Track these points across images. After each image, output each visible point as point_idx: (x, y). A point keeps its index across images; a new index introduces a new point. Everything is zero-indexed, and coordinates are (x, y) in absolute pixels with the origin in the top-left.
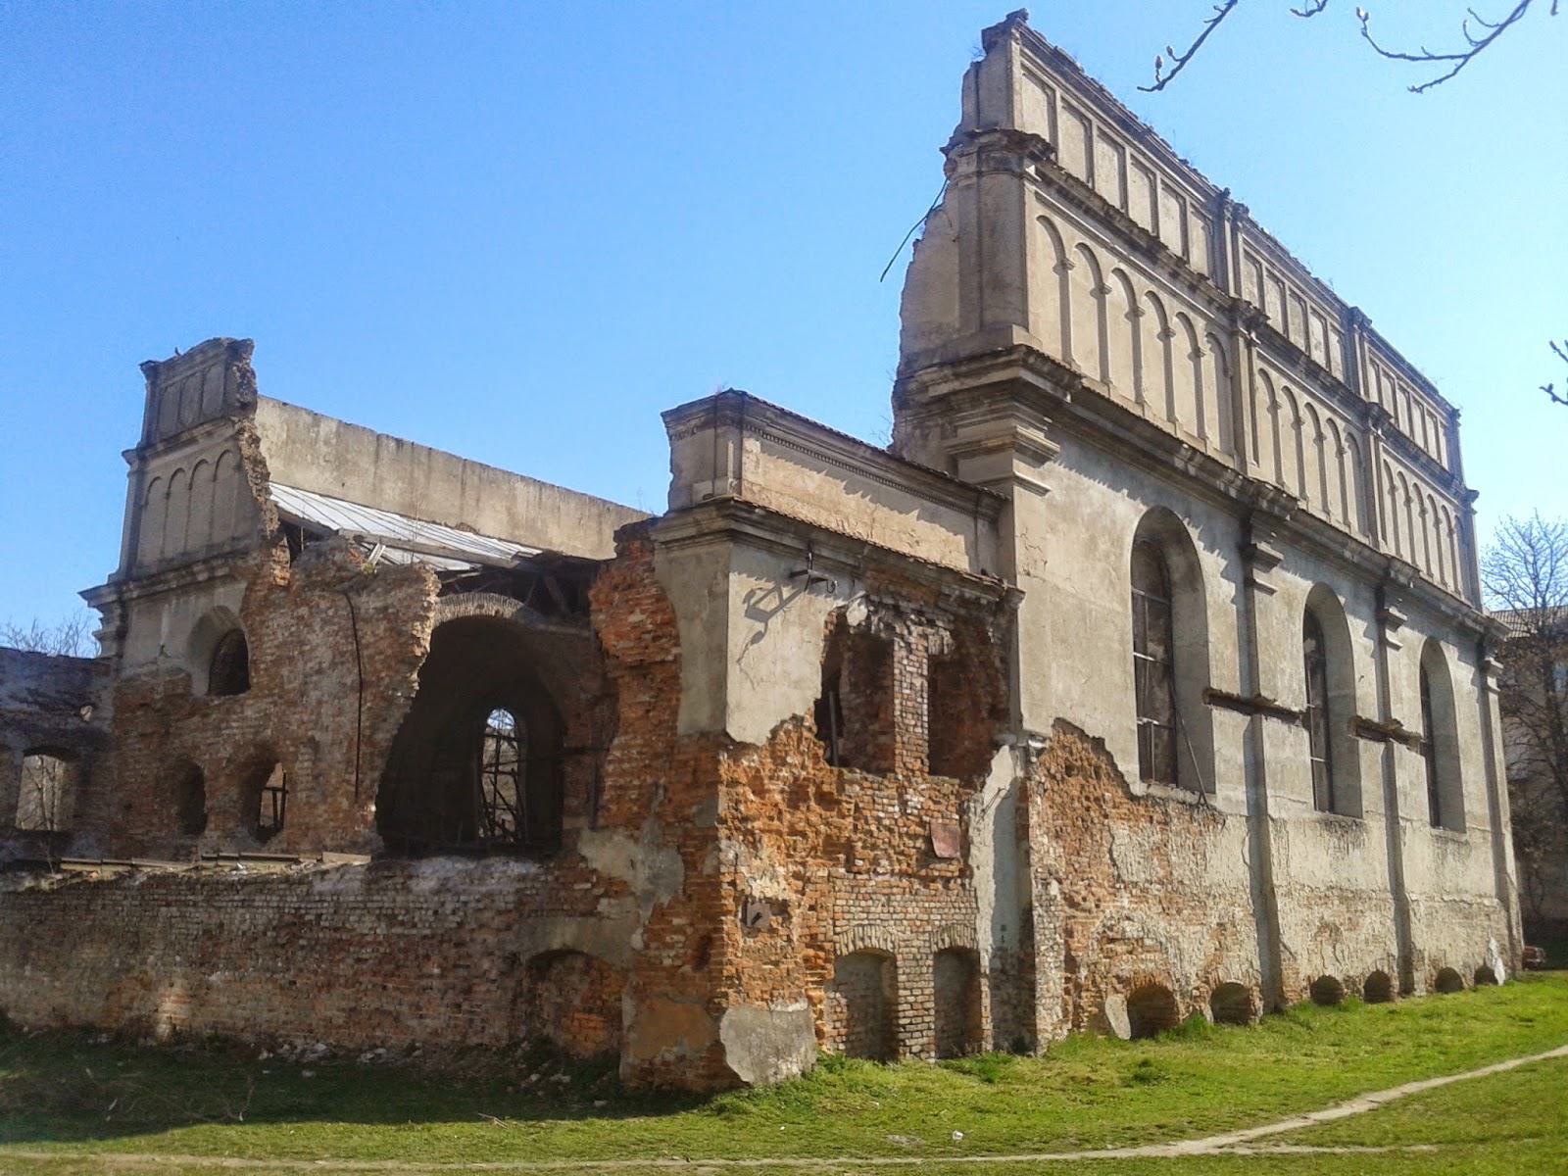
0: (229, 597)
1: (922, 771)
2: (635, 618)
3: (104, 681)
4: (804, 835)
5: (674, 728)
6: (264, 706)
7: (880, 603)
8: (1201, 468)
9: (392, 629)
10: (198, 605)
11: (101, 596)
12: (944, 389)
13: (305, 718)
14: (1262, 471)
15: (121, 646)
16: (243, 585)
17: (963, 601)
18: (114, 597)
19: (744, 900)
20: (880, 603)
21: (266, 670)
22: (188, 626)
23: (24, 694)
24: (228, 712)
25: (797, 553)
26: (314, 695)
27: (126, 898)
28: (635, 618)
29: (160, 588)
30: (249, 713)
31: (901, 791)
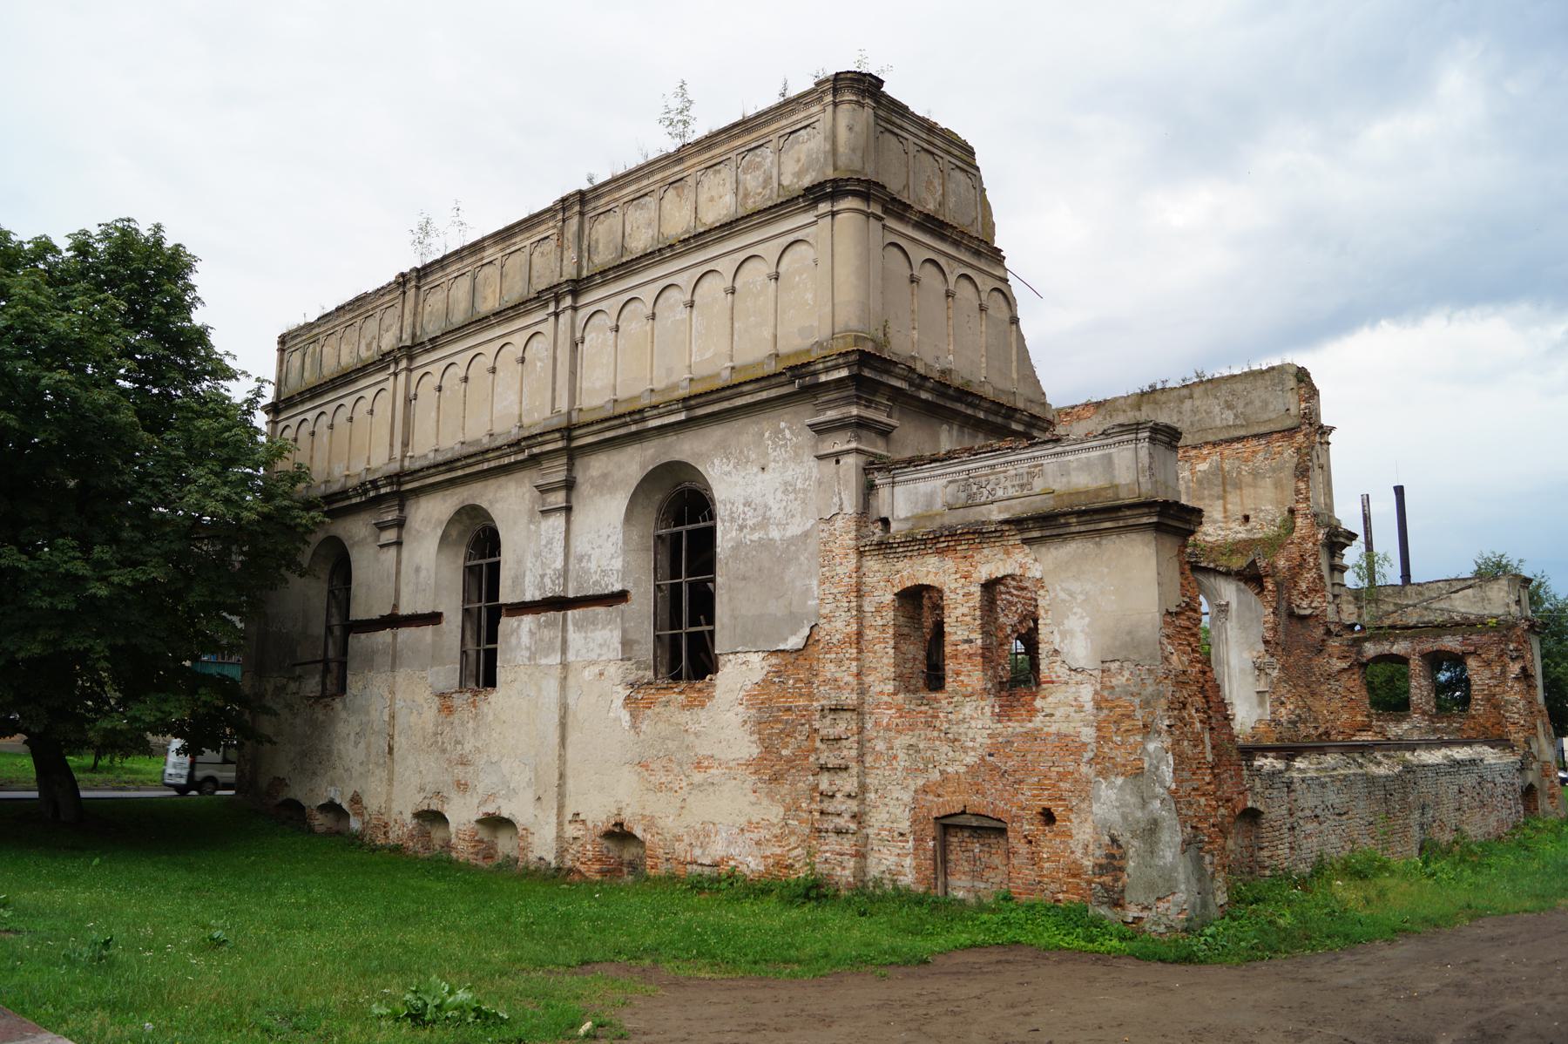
11: (889, 373)
18: (904, 385)
29: (961, 407)
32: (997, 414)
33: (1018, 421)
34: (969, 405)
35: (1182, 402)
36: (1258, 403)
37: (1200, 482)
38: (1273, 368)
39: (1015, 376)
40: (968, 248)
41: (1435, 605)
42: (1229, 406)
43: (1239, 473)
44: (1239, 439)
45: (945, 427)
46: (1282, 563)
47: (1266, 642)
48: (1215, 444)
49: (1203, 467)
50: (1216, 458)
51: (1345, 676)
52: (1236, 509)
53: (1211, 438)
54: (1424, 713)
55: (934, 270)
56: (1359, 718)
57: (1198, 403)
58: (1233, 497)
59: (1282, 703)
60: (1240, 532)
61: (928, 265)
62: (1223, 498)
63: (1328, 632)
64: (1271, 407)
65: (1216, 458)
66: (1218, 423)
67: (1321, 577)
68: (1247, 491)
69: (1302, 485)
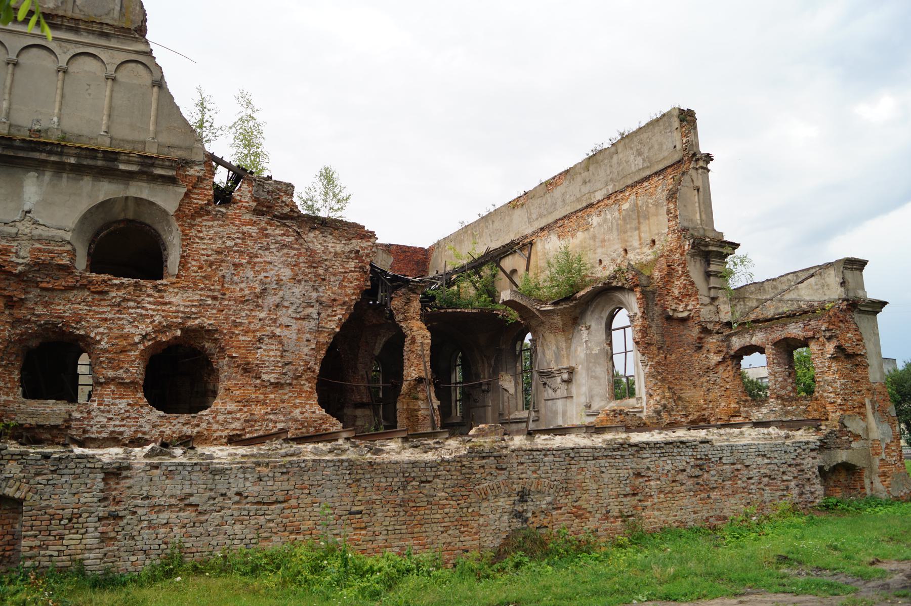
0: (167, 200)
2: (849, 335)
5: (866, 378)
6: (197, 297)
9: (361, 267)
10: (106, 190)
12: (714, 249)
13: (262, 315)
16: (184, 190)
21: (201, 268)
22: (84, 205)
26: (271, 300)
27: (545, 455)
28: (849, 335)
29: (37, 155)
30: (173, 300)
32: (95, 158)
33: (128, 162)
34: (50, 153)
35: (612, 158)
36: (656, 147)
37: (624, 219)
38: (664, 115)
39: (152, 128)
40: (92, 32)
41: (787, 297)
42: (640, 154)
43: (647, 206)
44: (647, 178)
45: (33, 174)
46: (656, 275)
47: (637, 343)
48: (633, 186)
49: (626, 206)
50: (633, 197)
51: (721, 368)
52: (647, 237)
53: (630, 182)
54: (779, 397)
55: (44, 53)
56: (733, 405)
57: (621, 156)
58: (644, 227)
59: (651, 395)
60: (648, 255)
61: (35, 50)
62: (638, 228)
63: (706, 331)
64: (665, 147)
65: (633, 197)
66: (633, 169)
67: (692, 283)
68: (653, 220)
69: (672, 206)
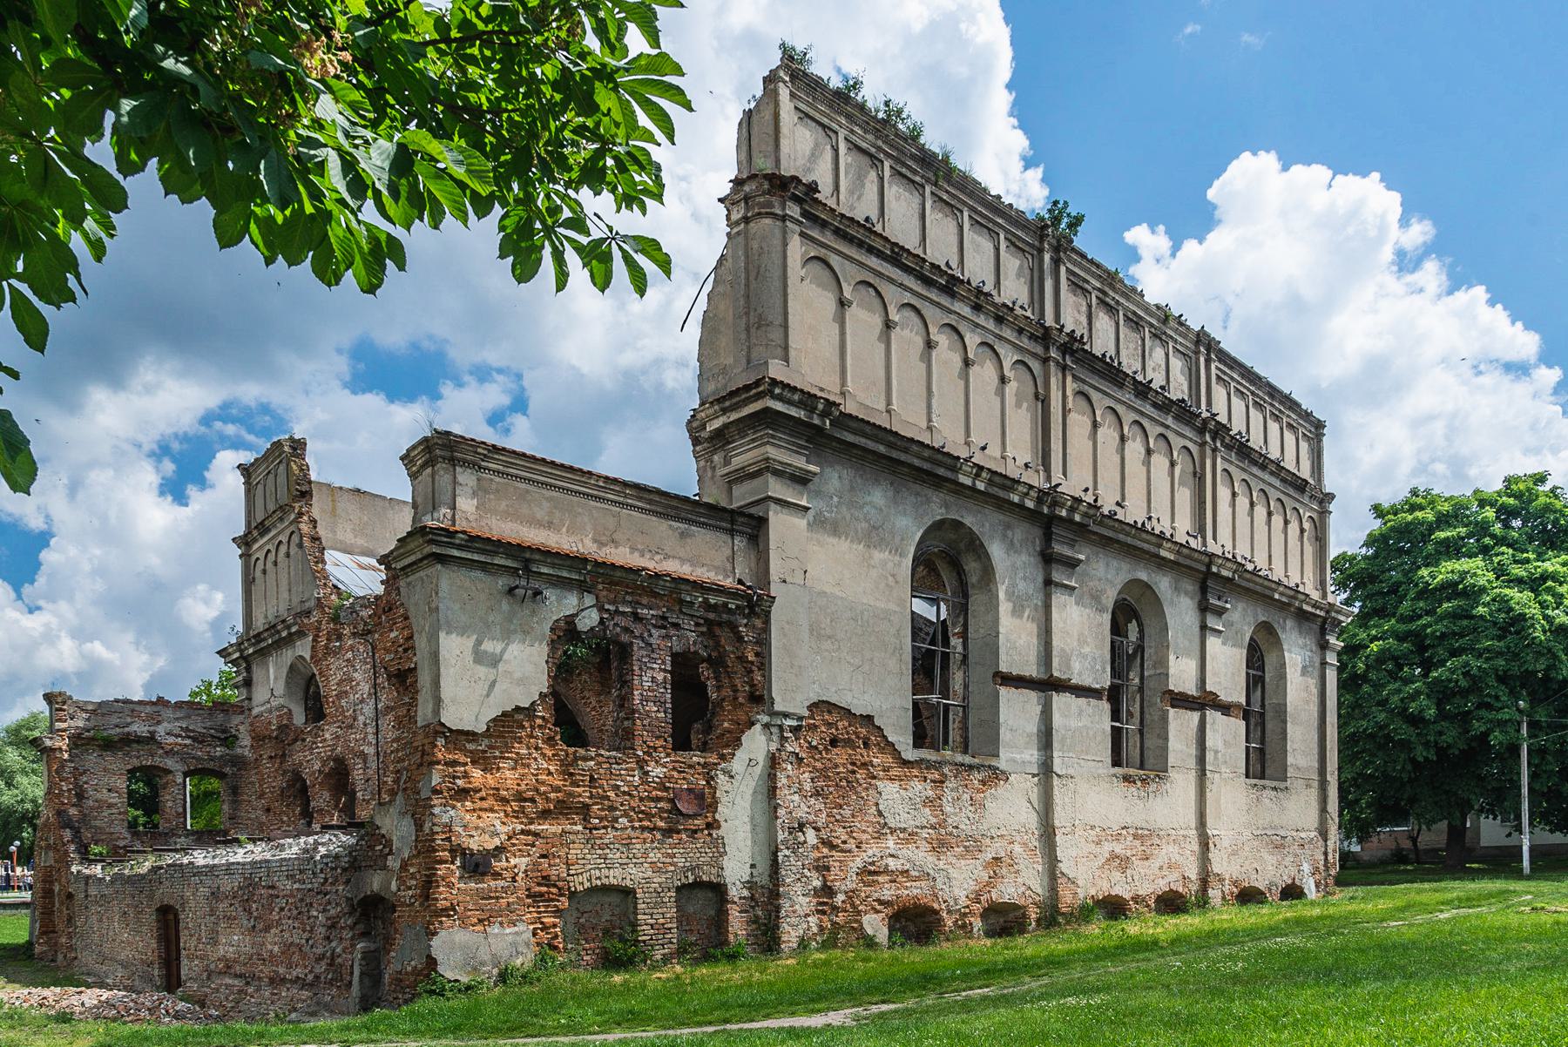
1: (664, 748)
3: (241, 718)
4: (533, 800)
7: (617, 612)
8: (990, 482)
14: (1073, 484)
15: (249, 692)
17: (707, 606)
19: (457, 851)
20: (617, 612)
23: (177, 731)
24: (317, 736)
25: (513, 572)
26: (361, 718)
30: (327, 736)
31: (641, 764)
